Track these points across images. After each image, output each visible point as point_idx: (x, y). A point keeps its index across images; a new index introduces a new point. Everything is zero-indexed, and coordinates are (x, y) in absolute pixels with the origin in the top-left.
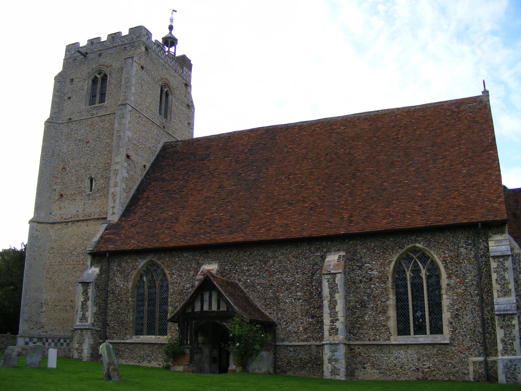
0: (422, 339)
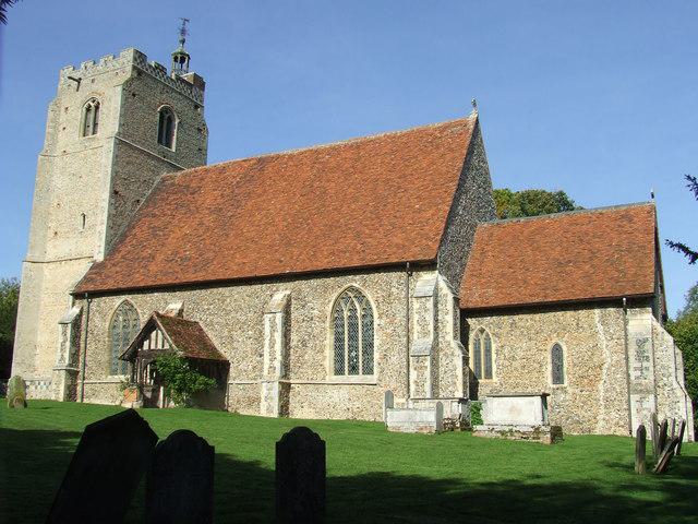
0: (354, 379)
